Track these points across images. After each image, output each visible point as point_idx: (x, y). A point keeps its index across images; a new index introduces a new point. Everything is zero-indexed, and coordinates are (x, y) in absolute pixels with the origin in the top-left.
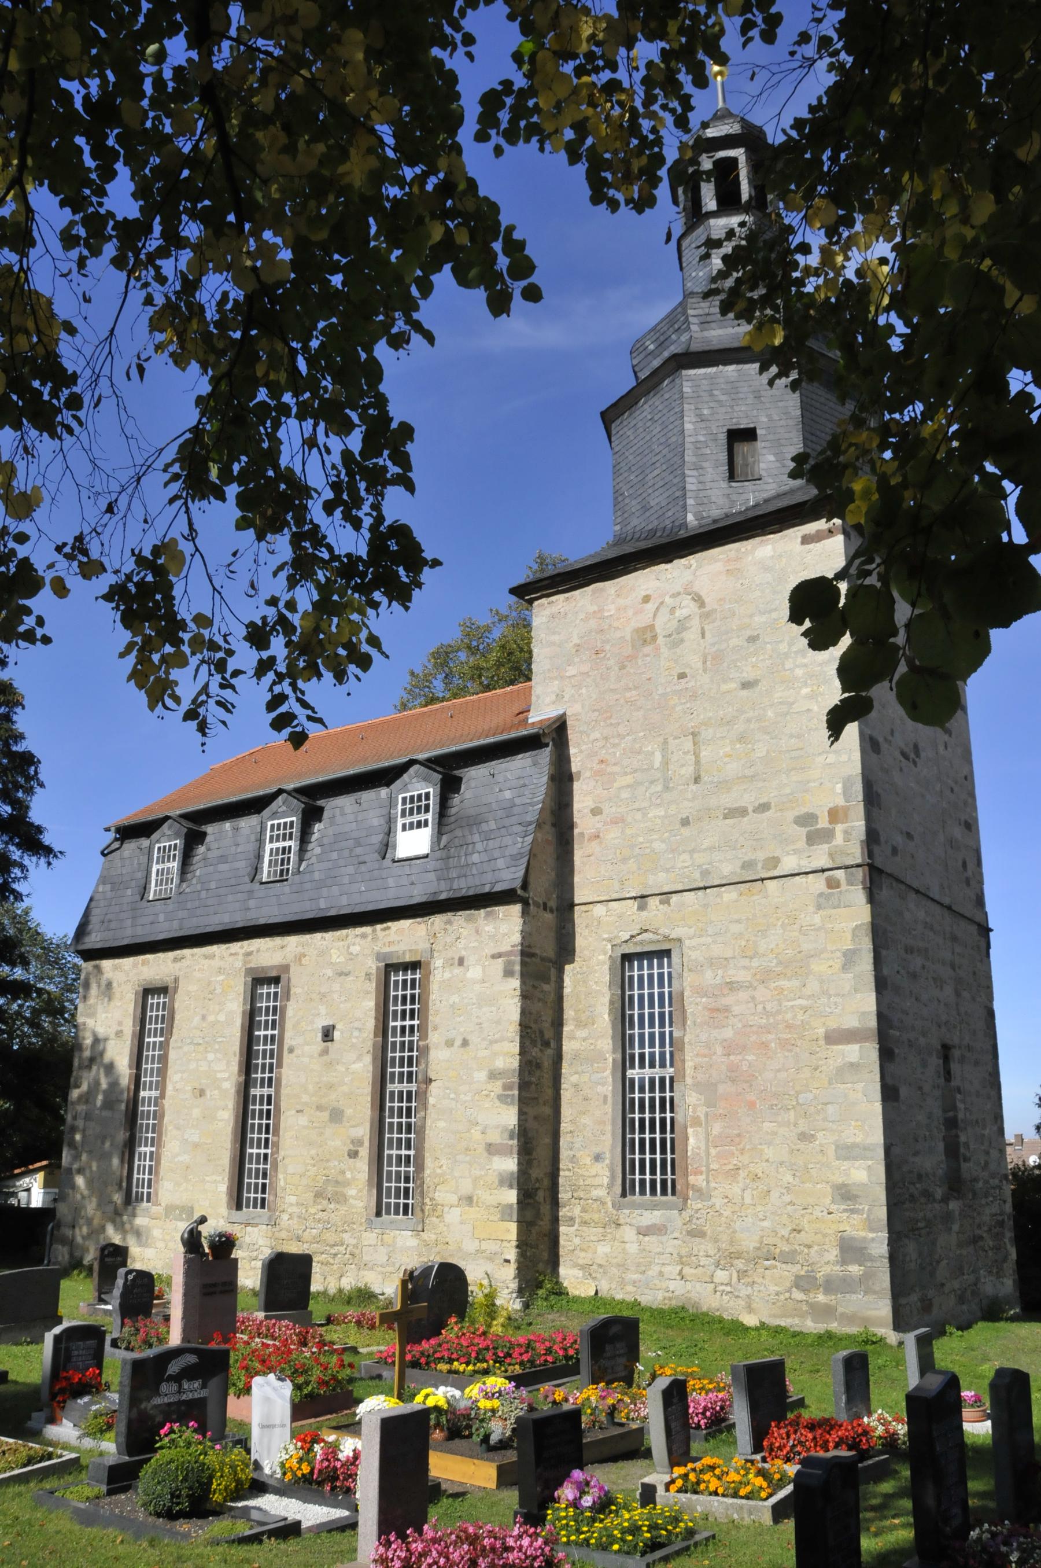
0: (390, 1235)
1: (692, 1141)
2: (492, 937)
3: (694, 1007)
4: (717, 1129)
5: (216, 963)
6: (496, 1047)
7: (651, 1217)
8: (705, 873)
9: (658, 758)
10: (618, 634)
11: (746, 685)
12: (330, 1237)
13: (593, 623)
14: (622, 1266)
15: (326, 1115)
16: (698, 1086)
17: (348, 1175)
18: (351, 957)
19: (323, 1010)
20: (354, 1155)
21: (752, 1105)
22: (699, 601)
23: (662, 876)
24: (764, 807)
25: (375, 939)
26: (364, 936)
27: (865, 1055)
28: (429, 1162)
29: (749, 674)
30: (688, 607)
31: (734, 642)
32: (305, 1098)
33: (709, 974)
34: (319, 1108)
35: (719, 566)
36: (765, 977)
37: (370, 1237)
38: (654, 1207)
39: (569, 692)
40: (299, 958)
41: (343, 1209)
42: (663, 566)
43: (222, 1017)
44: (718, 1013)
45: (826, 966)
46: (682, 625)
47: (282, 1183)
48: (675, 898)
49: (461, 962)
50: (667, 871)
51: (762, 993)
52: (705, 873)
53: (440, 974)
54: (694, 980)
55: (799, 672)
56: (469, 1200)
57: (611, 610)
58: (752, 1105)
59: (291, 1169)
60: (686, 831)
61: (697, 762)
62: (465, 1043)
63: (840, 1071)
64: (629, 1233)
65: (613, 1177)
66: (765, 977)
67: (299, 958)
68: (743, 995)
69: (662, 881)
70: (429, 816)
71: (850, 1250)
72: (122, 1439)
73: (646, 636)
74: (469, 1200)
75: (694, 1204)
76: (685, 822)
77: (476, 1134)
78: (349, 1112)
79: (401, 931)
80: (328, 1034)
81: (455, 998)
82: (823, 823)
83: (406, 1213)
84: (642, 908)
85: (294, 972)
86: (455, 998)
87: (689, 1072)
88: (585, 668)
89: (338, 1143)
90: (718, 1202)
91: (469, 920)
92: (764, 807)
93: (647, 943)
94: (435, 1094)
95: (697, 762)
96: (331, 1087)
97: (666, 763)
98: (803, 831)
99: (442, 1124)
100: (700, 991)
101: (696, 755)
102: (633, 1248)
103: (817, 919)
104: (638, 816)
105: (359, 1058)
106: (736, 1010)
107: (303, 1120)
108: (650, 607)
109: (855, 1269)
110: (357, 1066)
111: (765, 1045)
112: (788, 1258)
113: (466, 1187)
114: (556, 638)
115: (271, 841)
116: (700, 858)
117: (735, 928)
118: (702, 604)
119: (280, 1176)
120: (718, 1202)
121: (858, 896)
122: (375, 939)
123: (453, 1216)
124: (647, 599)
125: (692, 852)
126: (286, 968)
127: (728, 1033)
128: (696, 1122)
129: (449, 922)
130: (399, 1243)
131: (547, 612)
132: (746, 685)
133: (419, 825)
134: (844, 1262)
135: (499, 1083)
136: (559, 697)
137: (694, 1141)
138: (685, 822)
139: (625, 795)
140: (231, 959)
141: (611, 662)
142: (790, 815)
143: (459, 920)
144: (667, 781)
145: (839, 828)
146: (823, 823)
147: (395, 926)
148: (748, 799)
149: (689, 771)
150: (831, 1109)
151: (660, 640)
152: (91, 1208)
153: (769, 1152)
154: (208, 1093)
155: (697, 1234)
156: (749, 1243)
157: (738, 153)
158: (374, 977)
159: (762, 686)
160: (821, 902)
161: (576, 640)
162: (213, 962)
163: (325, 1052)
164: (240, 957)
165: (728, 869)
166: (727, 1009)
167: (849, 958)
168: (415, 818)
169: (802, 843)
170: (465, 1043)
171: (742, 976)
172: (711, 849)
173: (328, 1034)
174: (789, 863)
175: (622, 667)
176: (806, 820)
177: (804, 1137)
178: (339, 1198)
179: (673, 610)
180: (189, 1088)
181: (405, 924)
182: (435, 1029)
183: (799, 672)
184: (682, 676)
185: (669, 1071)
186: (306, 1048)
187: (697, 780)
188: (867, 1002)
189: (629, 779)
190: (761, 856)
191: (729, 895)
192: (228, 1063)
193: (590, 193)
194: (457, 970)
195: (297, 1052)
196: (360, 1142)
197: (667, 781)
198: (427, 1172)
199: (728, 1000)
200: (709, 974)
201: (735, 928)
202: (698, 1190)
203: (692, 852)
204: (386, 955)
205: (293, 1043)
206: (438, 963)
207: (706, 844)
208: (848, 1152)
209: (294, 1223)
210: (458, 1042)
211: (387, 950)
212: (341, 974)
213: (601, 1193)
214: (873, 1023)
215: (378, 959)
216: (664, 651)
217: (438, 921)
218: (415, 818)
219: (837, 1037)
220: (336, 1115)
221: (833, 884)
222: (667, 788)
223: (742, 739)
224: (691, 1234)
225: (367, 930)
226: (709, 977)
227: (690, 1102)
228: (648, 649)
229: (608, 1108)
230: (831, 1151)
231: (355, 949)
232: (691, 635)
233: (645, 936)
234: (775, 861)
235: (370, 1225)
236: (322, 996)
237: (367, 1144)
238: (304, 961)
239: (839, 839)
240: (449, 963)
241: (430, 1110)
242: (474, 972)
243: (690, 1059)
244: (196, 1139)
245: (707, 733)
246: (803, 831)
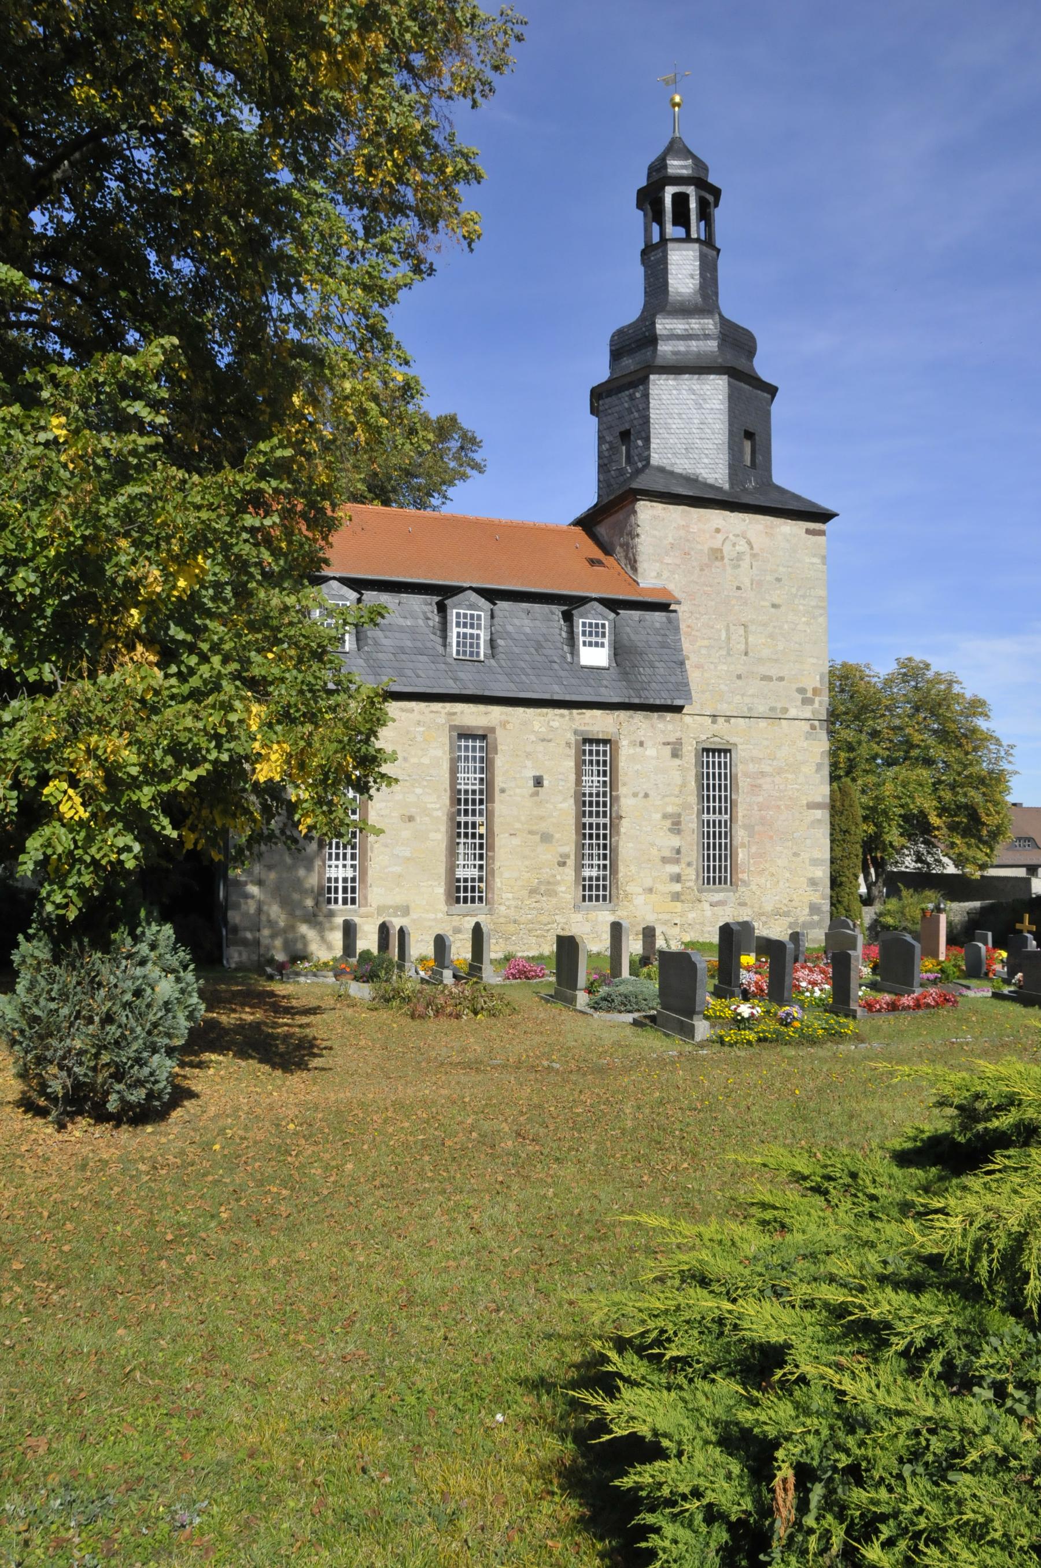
0: (593, 915)
1: (740, 856)
2: (663, 732)
3: (743, 783)
4: (753, 849)
5: (415, 716)
6: (667, 799)
7: (718, 897)
8: (750, 709)
9: (723, 636)
10: (699, 547)
11: (774, 606)
12: (544, 919)
13: (682, 533)
14: (702, 924)
15: (538, 838)
16: (745, 827)
17: (558, 877)
18: (552, 729)
19: (529, 763)
20: (563, 864)
21: (771, 837)
22: (749, 543)
23: (725, 706)
24: (781, 679)
25: (572, 719)
26: (562, 716)
27: (823, 815)
28: (622, 869)
29: (777, 601)
30: (742, 547)
31: (768, 578)
32: (518, 825)
33: (751, 766)
34: (531, 832)
35: (760, 527)
36: (780, 771)
37: (578, 917)
38: (721, 891)
39: (666, 574)
40: (504, 724)
41: (554, 900)
42: (728, 513)
43: (426, 761)
44: (755, 788)
45: (809, 769)
46: (740, 556)
47: (499, 885)
48: (733, 720)
49: (641, 744)
50: (729, 703)
51: (778, 779)
52: (750, 709)
53: (625, 750)
54: (743, 767)
55: (801, 608)
56: (650, 890)
57: (694, 529)
58: (771, 837)
59: (506, 875)
60: (739, 683)
61: (747, 643)
62: (646, 796)
63: (813, 822)
64: (706, 906)
65: (697, 876)
66: (780, 771)
67: (504, 724)
68: (768, 779)
69: (724, 708)
70: (606, 641)
71: (814, 909)
72: (853, 974)
73: (717, 555)
74: (650, 890)
75: (741, 889)
76: (739, 677)
77: (654, 851)
78: (557, 836)
79: (593, 717)
80: (538, 782)
81: (638, 767)
82: (809, 694)
83: (604, 899)
84: (714, 722)
85: (499, 732)
86: (638, 767)
87: (740, 818)
88: (678, 561)
89: (549, 857)
90: (754, 887)
91: (645, 718)
92: (781, 679)
93: (716, 743)
94: (625, 826)
95: (747, 643)
96: (542, 818)
97: (728, 639)
98: (800, 697)
99: (630, 845)
100: (746, 775)
101: (746, 639)
102: (708, 913)
103: (805, 744)
104: (712, 667)
105: (565, 800)
106: (765, 787)
107: (516, 841)
108: (720, 537)
109: (816, 918)
110: (565, 805)
111: (779, 807)
112: (786, 914)
113: (648, 883)
114: (656, 533)
115: (458, 625)
116: (747, 700)
117: (765, 743)
118: (752, 548)
119: (497, 880)
120: (754, 887)
121: (823, 735)
122: (572, 719)
123: (639, 900)
124: (718, 531)
125: (743, 695)
126: (493, 730)
127: (760, 799)
128: (743, 845)
129: (631, 717)
130: (600, 918)
131: (650, 512)
132: (774, 606)
133: (597, 644)
134: (811, 914)
135: (669, 821)
136: (659, 575)
137: (741, 855)
138: (739, 677)
139: (704, 651)
140: (432, 715)
141: (695, 564)
142: (795, 686)
143: (639, 716)
144: (729, 650)
145: (817, 699)
146: (809, 694)
147: (589, 713)
148: (774, 672)
149: (742, 647)
150: (808, 841)
151: (726, 561)
152: (275, 911)
153: (779, 862)
154: (418, 819)
155: (743, 904)
156: (768, 908)
157: (691, 190)
158: (573, 746)
159: (783, 609)
160: (808, 736)
161: (670, 540)
162: (411, 716)
163: (537, 794)
164: (443, 715)
165: (761, 709)
166: (760, 786)
167: (819, 767)
168: (594, 639)
169: (799, 703)
170: (646, 796)
171: (767, 769)
172: (753, 696)
173: (538, 782)
174: (793, 713)
175: (702, 570)
176: (802, 691)
177: (796, 855)
178: (551, 893)
179: (734, 545)
180: (395, 814)
181: (597, 713)
182: (624, 784)
183: (801, 608)
184: (739, 588)
185: (705, 817)
186: (518, 791)
187: (746, 654)
188: (826, 790)
189: (706, 643)
190: (779, 705)
191: (763, 724)
192: (439, 797)
193: (643, 183)
194: (639, 749)
195: (508, 792)
196: (567, 856)
197: (729, 650)
198: (620, 875)
199: (760, 781)
200: (751, 766)
201: (765, 743)
202: (743, 881)
203: (743, 695)
204: (582, 732)
205: (503, 785)
206: (624, 743)
207: (750, 692)
208: (815, 862)
209: (512, 913)
210: (641, 795)
211: (582, 728)
212: (543, 740)
213: (691, 884)
214: (828, 800)
215: (576, 732)
216: (729, 570)
217: (623, 715)
218: (594, 639)
219: (812, 806)
220: (546, 838)
221: (813, 727)
222: (728, 654)
223: (771, 636)
224: (740, 904)
225: (565, 712)
226: (752, 768)
227: (740, 835)
228: (717, 563)
229: (695, 836)
230: (807, 861)
231: (555, 724)
232: (745, 564)
233: (716, 739)
234: (785, 710)
235: (576, 908)
236: (528, 755)
237: (573, 857)
238: (508, 726)
239: (816, 705)
240: (633, 743)
241: (622, 836)
242: (651, 752)
243: (741, 812)
244: (408, 854)
245: (752, 628)
246: (800, 697)
